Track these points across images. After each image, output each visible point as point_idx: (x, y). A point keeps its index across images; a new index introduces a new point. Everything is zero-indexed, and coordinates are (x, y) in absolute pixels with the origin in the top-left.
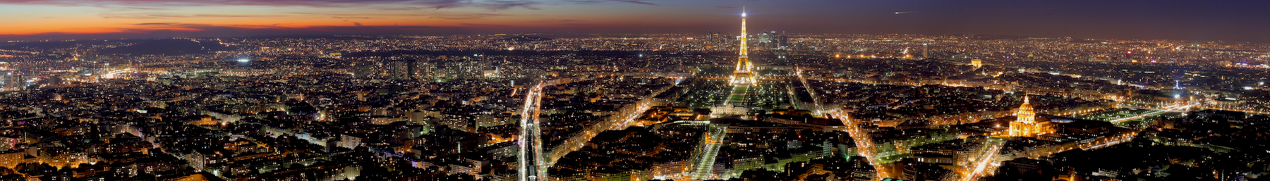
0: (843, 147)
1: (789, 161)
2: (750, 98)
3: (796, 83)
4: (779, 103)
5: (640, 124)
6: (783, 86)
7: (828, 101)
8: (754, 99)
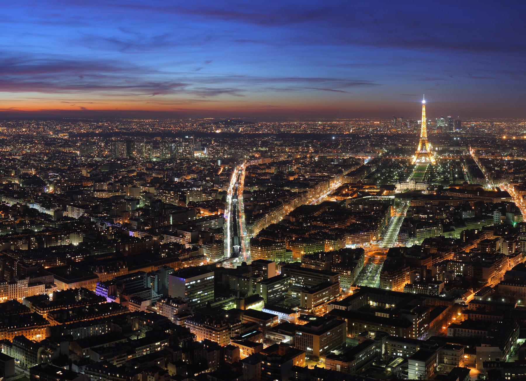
0: (510, 215)
1: (465, 229)
2: (428, 174)
3: (469, 161)
4: (455, 179)
5: (333, 200)
6: (458, 164)
7: (497, 177)
8: (433, 176)
